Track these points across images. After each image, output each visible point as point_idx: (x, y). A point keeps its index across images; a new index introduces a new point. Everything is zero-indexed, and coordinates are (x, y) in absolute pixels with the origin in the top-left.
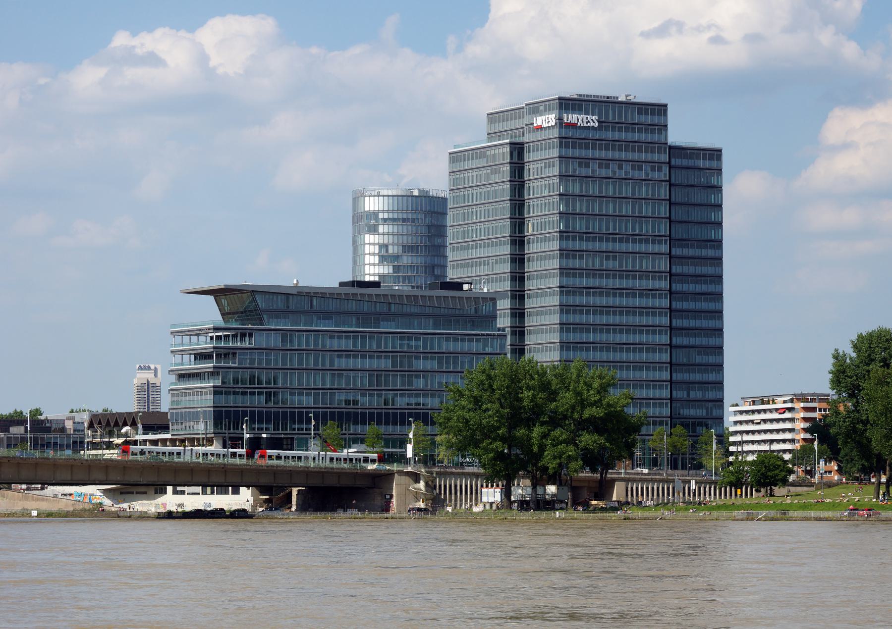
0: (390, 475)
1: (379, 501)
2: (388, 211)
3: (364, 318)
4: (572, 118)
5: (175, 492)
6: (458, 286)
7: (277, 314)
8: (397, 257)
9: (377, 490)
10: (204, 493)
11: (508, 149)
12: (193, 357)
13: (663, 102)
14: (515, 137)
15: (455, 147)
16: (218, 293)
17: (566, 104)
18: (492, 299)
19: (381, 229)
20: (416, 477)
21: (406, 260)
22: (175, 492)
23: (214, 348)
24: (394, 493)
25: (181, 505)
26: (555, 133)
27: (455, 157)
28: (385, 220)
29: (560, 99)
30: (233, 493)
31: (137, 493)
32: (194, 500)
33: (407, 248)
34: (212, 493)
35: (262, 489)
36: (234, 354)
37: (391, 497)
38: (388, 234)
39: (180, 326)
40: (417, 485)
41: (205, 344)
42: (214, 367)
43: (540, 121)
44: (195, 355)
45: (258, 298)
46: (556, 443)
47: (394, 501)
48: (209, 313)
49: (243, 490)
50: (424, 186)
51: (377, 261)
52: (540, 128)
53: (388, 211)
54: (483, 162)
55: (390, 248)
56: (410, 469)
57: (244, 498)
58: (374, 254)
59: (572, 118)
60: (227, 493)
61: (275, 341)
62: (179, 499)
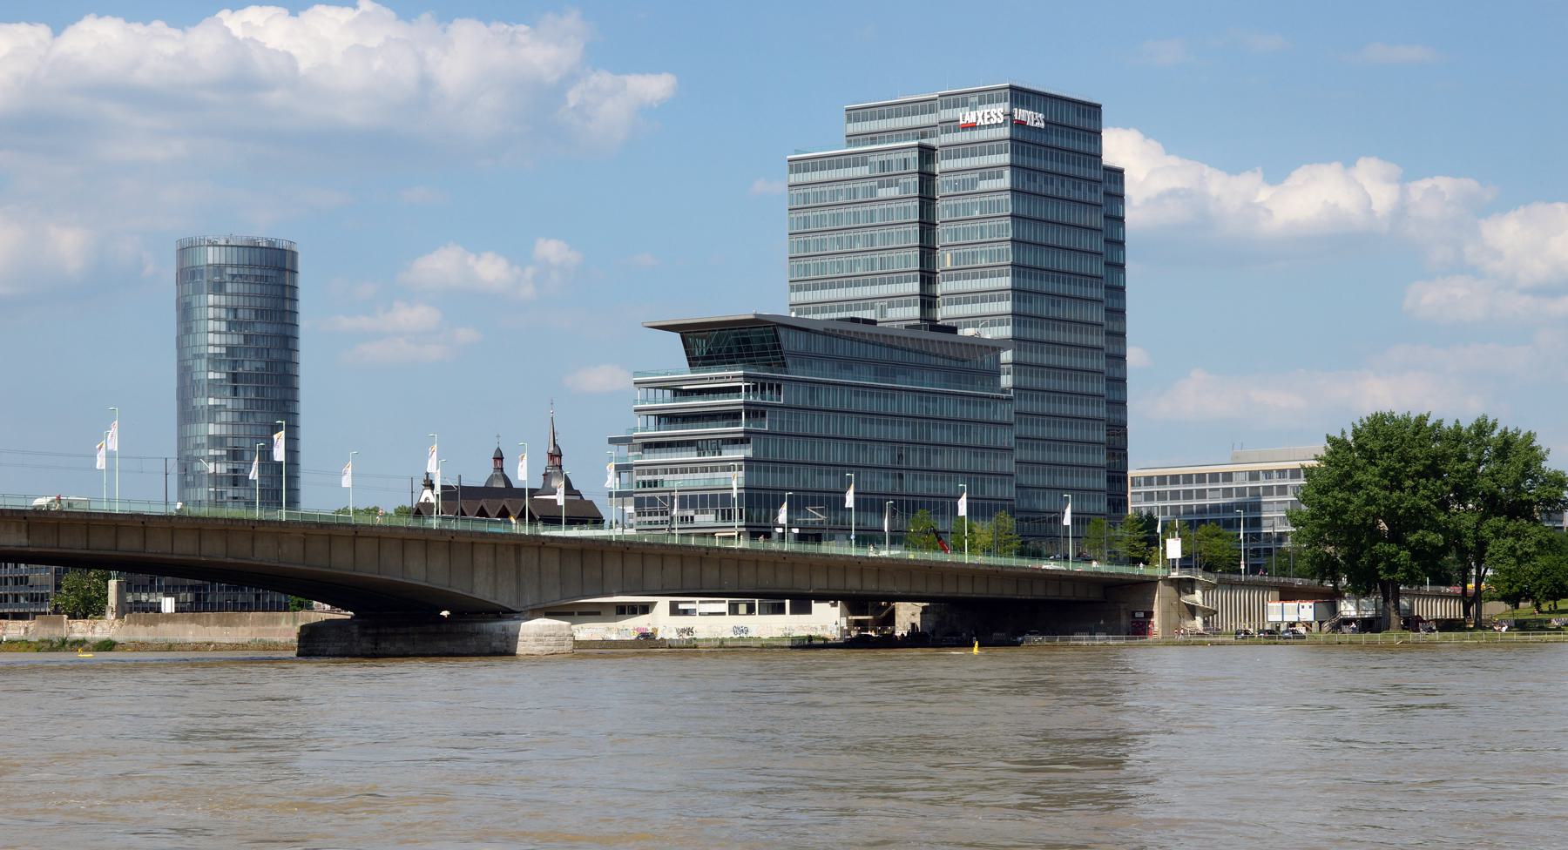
0: (1149, 584)
1: (1125, 622)
2: (238, 266)
3: (885, 368)
4: (1022, 114)
5: (674, 610)
6: (953, 330)
7: (806, 358)
8: (249, 323)
9: (1122, 606)
10: (734, 610)
11: (916, 154)
12: (652, 419)
13: (1095, 101)
14: (924, 136)
15: (797, 152)
16: (688, 332)
17: (1020, 96)
18: (995, 347)
19: (229, 288)
20: (1185, 586)
21: (259, 328)
22: (674, 610)
23: (745, 404)
24: (1156, 609)
25: (690, 631)
26: (1005, 132)
27: (797, 166)
28: (233, 276)
29: (1011, 88)
30: (795, 610)
31: (580, 614)
32: (712, 621)
33: (261, 313)
34: (750, 610)
35: (854, 603)
36: (763, 415)
37: (1150, 614)
38: (238, 295)
39: (645, 374)
40: (1190, 597)
41: (666, 402)
42: (745, 432)
43: (969, 117)
44: (660, 416)
45: (782, 333)
46: (1497, 533)
47: (1156, 620)
48: (672, 359)
49: (815, 606)
50: (273, 236)
51: (224, 329)
52: (973, 127)
53: (238, 266)
54: (864, 171)
55: (241, 314)
56: (1175, 575)
57: (827, 619)
58: (220, 320)
59: (1022, 114)
60: (780, 610)
61: (801, 397)
62: (683, 621)
